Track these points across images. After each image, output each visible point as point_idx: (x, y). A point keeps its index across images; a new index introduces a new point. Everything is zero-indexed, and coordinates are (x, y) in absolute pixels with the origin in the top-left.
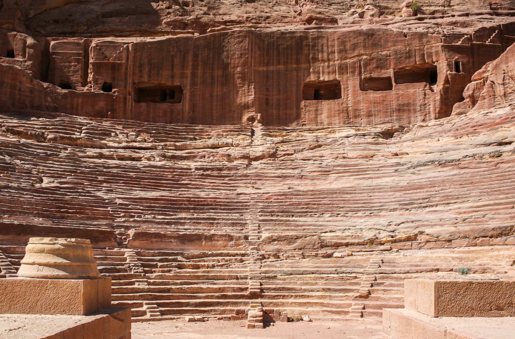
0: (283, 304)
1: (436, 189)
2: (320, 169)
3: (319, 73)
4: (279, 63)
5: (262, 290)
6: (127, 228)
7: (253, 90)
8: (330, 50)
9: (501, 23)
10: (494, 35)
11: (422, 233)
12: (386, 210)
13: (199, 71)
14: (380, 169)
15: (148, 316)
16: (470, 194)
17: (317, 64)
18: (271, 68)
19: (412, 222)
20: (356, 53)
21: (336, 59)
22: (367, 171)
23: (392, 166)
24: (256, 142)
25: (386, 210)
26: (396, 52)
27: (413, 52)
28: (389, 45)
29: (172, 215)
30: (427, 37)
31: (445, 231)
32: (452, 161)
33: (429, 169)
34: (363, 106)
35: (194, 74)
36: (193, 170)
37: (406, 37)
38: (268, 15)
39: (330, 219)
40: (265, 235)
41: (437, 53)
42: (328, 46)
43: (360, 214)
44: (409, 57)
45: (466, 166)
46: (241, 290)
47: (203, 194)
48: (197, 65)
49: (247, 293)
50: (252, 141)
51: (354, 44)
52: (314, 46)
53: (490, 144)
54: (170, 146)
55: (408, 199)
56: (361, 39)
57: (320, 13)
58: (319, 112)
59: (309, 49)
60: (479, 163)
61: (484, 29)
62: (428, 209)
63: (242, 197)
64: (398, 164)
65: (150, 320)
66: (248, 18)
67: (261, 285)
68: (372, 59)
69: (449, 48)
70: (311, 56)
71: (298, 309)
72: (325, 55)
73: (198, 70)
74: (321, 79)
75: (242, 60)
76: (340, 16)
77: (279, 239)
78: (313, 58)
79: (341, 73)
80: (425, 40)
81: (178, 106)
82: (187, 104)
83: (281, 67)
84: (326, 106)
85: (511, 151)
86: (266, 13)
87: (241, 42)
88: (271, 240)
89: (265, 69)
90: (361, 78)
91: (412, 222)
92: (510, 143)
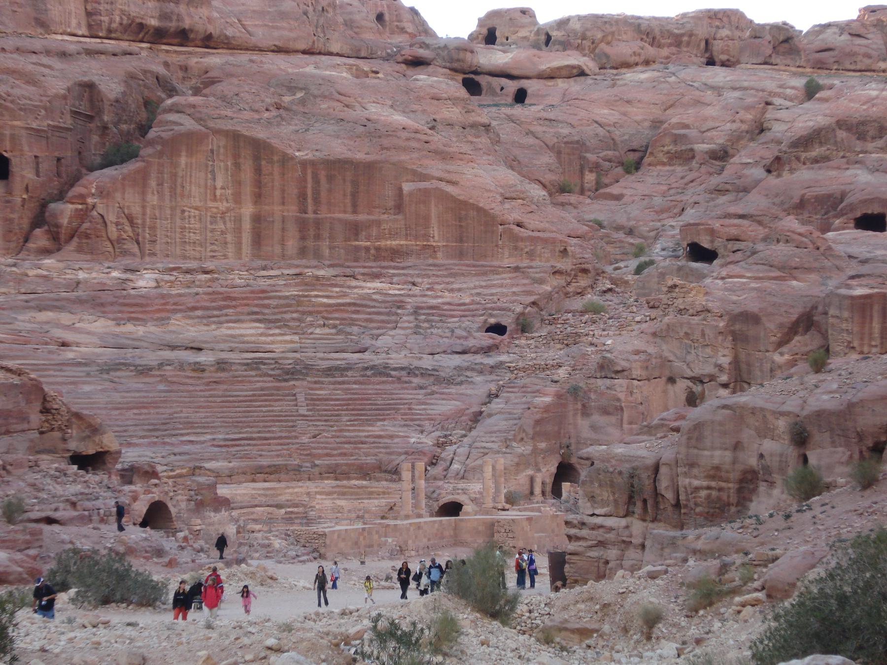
1: (169, 411)
11: (200, 468)
12: (136, 436)
14: (65, 368)
16: (213, 422)
19: (180, 454)
22: (49, 370)
25: (136, 436)
32: (151, 369)
41: (13, 137)
45: (174, 379)
53: (173, 348)
55: (146, 422)
61: (56, 96)
64: (79, 364)
85: (212, 366)
91: (180, 454)
92: (200, 349)
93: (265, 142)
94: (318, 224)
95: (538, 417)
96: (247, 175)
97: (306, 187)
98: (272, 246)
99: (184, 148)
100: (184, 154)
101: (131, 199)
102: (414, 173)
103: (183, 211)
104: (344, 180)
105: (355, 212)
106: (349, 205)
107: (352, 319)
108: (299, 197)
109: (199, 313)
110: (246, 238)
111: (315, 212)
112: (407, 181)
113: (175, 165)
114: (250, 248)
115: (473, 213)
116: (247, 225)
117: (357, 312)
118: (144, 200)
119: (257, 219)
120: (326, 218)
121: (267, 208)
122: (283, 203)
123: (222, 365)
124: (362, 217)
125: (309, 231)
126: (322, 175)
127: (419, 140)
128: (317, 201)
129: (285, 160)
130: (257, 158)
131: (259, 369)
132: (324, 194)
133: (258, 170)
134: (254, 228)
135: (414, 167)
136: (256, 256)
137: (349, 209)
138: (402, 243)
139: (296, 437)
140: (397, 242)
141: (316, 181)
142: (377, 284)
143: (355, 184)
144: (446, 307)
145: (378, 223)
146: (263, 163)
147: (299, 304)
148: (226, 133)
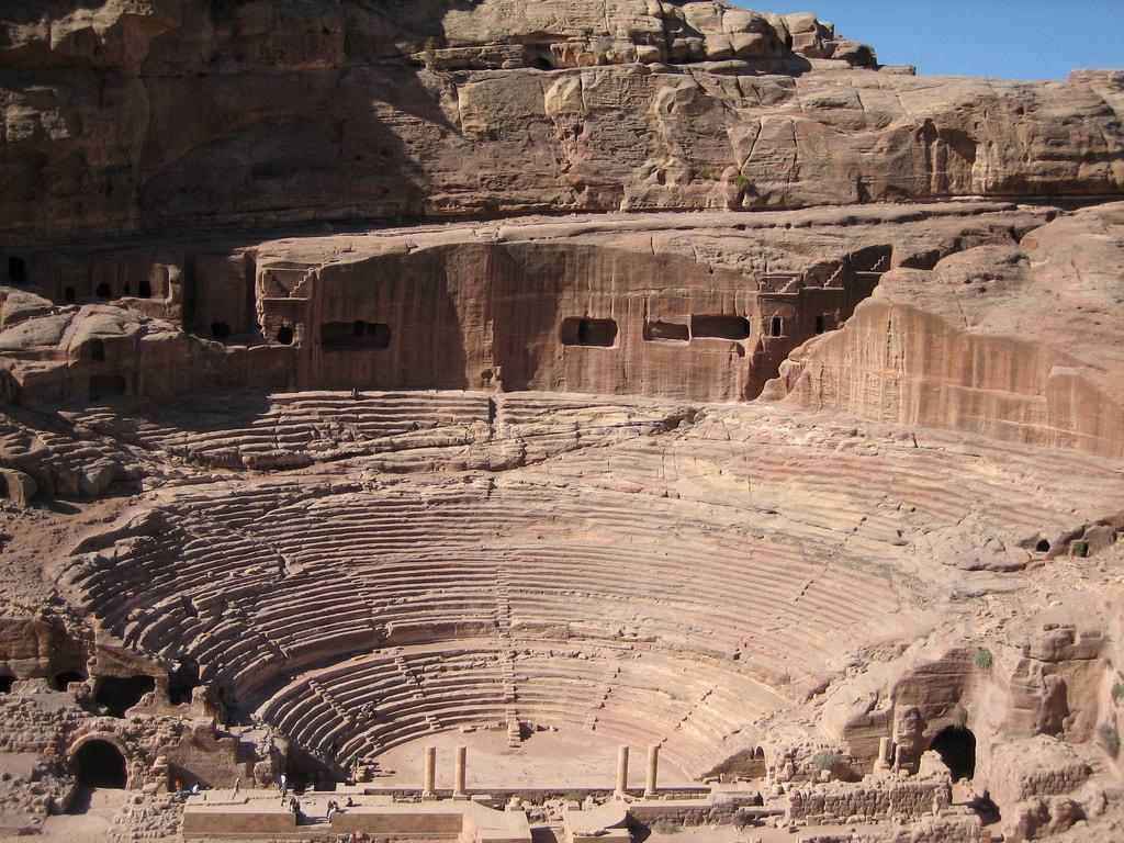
0: (533, 711)
2: (577, 506)
3: (586, 306)
4: (530, 289)
5: (516, 696)
6: (384, 622)
7: (491, 332)
8: (604, 276)
9: (851, 251)
10: (836, 272)
13: (415, 303)
14: (644, 518)
15: (432, 728)
17: (585, 293)
18: (518, 297)
20: (641, 286)
21: (613, 288)
23: (657, 516)
24: (498, 435)
26: (697, 293)
27: (720, 296)
28: (689, 280)
29: (423, 593)
30: (741, 278)
31: (680, 639)
33: (693, 534)
34: (646, 363)
35: (407, 309)
36: (425, 505)
37: (712, 272)
38: (516, 171)
39: (580, 600)
40: (515, 622)
41: (751, 303)
42: (602, 269)
43: (609, 597)
44: (714, 302)
46: (498, 695)
47: (444, 552)
48: (413, 295)
49: (504, 698)
50: (493, 431)
51: (639, 273)
52: (582, 267)
54: (386, 444)
56: (651, 266)
57: (597, 173)
58: (584, 364)
59: (574, 272)
60: (740, 542)
62: (673, 604)
63: (489, 556)
65: (434, 733)
66: (483, 180)
67: (515, 689)
68: (662, 297)
69: (768, 300)
70: (577, 281)
71: (545, 717)
72: (598, 280)
73: (413, 300)
74: (590, 315)
75: (477, 289)
76: (628, 177)
77: (529, 626)
78: (579, 284)
79: (619, 311)
80: (736, 282)
81: (384, 354)
82: (397, 351)
83: (534, 296)
84: (595, 353)
86: (513, 166)
87: (478, 261)
88: (521, 627)
89: (509, 298)
90: (645, 321)
93: (936, 316)
94: (977, 398)
95: (909, 676)
96: (919, 347)
97: (971, 361)
98: (937, 414)
99: (870, 318)
100: (869, 324)
101: (833, 363)
102: (1065, 357)
103: (868, 376)
104: (1005, 357)
105: (1013, 389)
106: (1009, 382)
107: (926, 507)
108: (964, 370)
109: (811, 477)
110: (916, 403)
111: (979, 386)
112: (1057, 365)
113: (863, 334)
114: (917, 414)
115: (1109, 407)
116: (916, 394)
117: (937, 499)
118: (842, 363)
119: (925, 388)
120: (982, 393)
121: (935, 378)
122: (949, 376)
123: (779, 536)
124: (1016, 396)
125: (970, 406)
126: (987, 350)
127: (1089, 322)
128: (981, 376)
129: (955, 335)
130: (928, 332)
131: (801, 545)
132: (987, 369)
133: (929, 343)
134: (922, 396)
135: (1066, 351)
136: (922, 423)
137: (1009, 386)
138: (1047, 427)
139: (761, 627)
140: (1042, 426)
141: (982, 358)
142: (992, 470)
143: (1014, 361)
144: (1023, 510)
145: (1028, 404)
146: (934, 336)
147: (895, 482)
148: (902, 308)
